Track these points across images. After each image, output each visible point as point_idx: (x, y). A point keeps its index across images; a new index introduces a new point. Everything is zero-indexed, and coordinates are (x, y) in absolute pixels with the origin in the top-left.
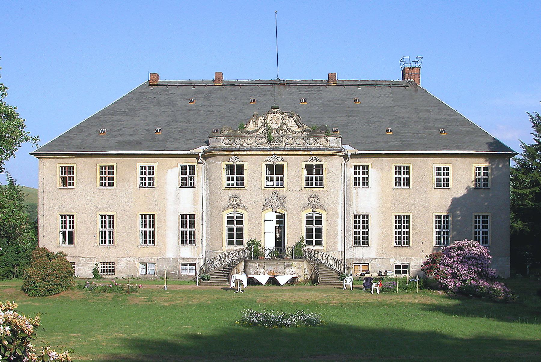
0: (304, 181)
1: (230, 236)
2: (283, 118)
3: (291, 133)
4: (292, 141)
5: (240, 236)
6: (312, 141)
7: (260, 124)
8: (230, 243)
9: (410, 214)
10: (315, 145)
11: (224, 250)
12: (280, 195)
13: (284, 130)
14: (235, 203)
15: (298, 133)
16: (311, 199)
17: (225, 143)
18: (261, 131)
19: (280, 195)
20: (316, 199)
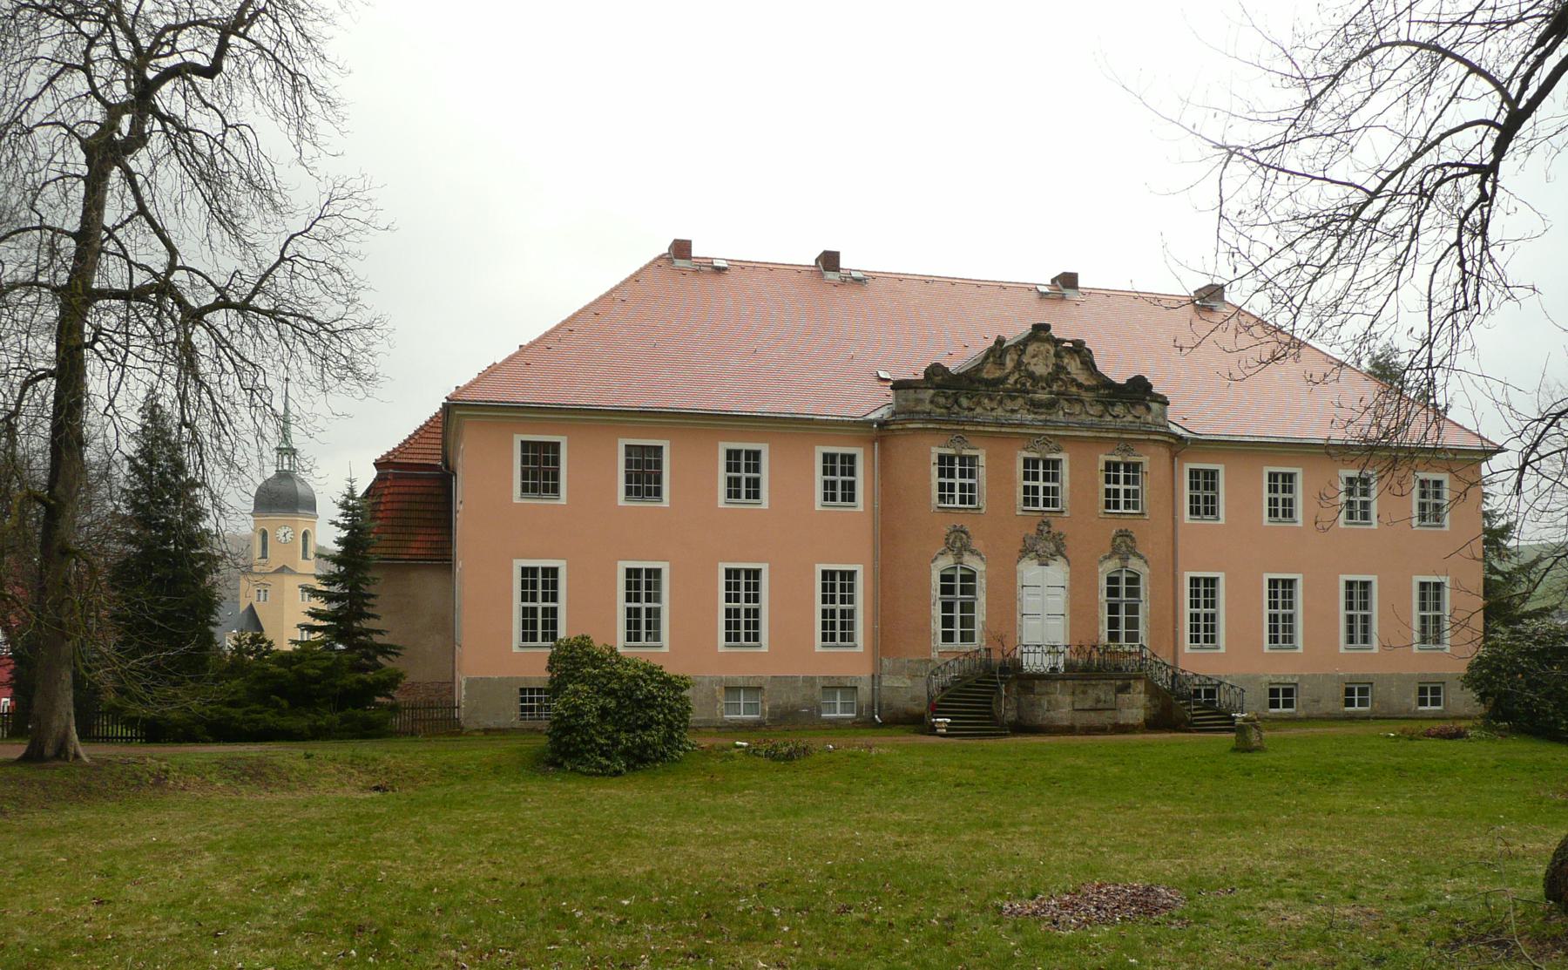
0: (1020, 496)
1: (948, 622)
2: (1057, 355)
3: (1074, 389)
4: (1077, 408)
5: (967, 622)
6: (1119, 409)
7: (1009, 363)
8: (948, 637)
9: (1267, 577)
10: (1125, 419)
11: (935, 655)
12: (1054, 530)
13: (1061, 380)
14: (958, 544)
15: (1088, 389)
16: (1118, 540)
17: (938, 405)
18: (1011, 380)
19: (1054, 530)
20: (1128, 540)
